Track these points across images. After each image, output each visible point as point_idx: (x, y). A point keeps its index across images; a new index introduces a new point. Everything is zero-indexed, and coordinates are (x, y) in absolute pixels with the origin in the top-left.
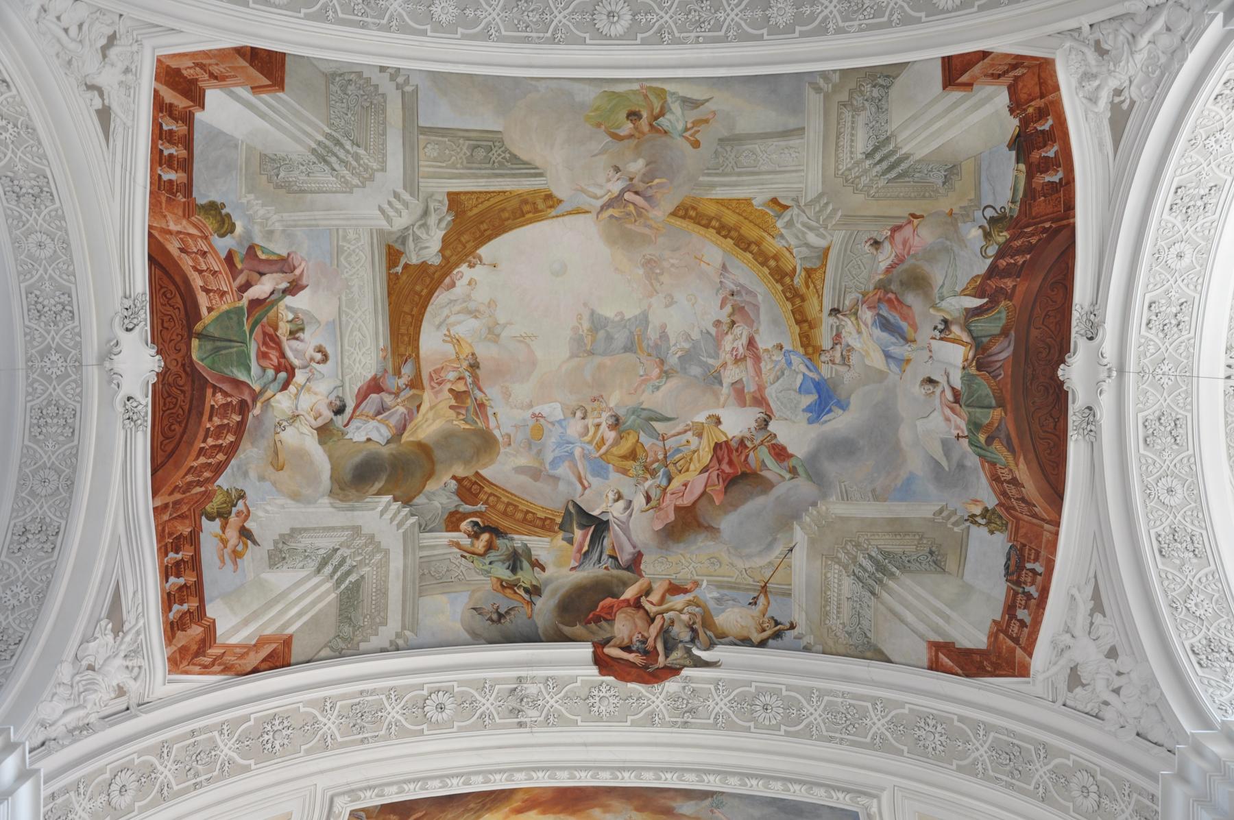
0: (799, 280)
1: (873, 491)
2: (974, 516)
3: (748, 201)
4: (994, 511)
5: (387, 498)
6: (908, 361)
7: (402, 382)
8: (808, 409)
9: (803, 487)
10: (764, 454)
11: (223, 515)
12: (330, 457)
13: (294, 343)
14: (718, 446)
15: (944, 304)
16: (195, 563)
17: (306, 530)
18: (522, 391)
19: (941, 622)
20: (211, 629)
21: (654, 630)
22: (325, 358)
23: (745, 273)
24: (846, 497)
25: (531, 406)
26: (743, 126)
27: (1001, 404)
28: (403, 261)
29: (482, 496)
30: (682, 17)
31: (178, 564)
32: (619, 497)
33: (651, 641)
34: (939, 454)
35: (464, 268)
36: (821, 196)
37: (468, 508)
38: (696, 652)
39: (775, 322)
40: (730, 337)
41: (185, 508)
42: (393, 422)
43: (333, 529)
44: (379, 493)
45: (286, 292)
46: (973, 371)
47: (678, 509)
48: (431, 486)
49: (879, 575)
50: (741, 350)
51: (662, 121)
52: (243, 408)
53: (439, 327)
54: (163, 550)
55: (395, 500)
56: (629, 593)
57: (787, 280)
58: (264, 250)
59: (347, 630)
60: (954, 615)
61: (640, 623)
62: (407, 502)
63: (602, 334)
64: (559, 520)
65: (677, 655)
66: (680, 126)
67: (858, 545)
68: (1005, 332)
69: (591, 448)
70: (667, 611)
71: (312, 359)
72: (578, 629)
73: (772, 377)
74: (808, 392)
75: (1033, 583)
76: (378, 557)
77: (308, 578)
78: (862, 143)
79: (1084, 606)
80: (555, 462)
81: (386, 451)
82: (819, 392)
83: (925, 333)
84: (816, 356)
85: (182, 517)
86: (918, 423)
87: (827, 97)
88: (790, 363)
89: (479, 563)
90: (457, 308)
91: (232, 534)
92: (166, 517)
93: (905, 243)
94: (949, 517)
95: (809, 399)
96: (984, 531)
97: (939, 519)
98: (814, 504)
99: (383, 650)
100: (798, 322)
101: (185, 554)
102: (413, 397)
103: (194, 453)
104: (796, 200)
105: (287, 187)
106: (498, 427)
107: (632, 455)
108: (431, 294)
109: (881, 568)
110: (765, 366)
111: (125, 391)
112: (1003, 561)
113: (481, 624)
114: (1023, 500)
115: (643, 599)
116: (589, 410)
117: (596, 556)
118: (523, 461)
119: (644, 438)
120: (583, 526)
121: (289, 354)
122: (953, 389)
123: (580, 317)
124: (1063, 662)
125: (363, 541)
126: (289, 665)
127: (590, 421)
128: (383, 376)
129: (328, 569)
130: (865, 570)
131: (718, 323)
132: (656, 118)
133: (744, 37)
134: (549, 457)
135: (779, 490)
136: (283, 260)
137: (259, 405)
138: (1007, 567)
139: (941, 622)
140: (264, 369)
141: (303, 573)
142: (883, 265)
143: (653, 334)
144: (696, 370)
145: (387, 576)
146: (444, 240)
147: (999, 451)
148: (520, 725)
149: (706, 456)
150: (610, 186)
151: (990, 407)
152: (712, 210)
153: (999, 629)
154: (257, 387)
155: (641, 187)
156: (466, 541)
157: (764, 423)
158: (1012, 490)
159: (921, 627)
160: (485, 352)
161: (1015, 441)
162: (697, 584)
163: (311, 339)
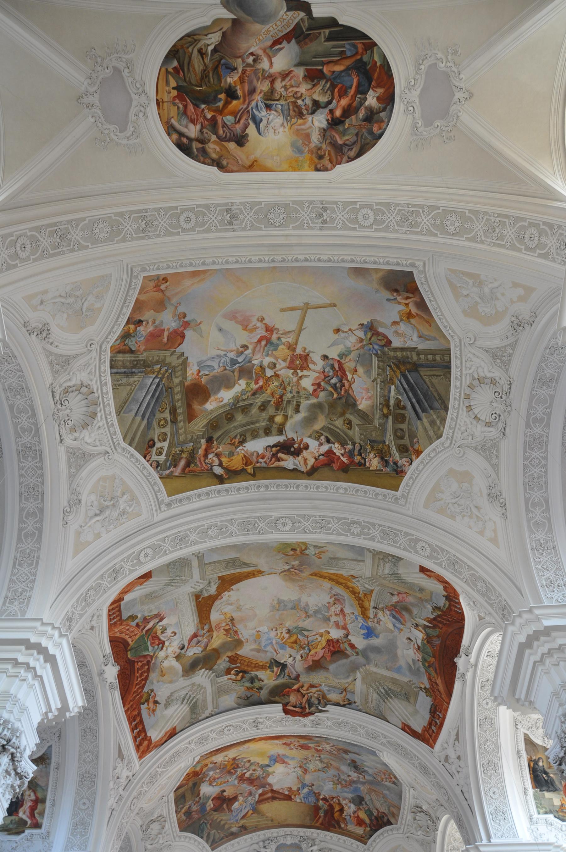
0: (361, 595)
1: (387, 667)
2: (421, 688)
3: (342, 575)
4: (428, 689)
5: (204, 670)
6: (402, 630)
7: (204, 632)
8: (363, 634)
9: (360, 659)
10: (346, 645)
11: (147, 701)
12: (181, 665)
13: (164, 635)
14: (328, 641)
15: (416, 619)
16: (141, 722)
17: (175, 691)
18: (251, 625)
19: (406, 718)
20: (150, 740)
21: (304, 700)
22: (175, 634)
23: (339, 590)
24: (376, 666)
25: (255, 628)
26: (339, 555)
27: (434, 657)
28: (202, 597)
29: (239, 661)
30: (314, 525)
31: (136, 725)
32: (291, 656)
33: (303, 704)
34: (411, 663)
35: (226, 593)
36: (370, 578)
37: (234, 666)
38: (320, 708)
39: (352, 606)
40: (333, 607)
41: (135, 706)
42: (203, 645)
43: (185, 687)
44: (200, 669)
45: (158, 622)
46: (425, 642)
47: (313, 661)
48: (219, 662)
49: (387, 696)
50: (338, 612)
51: (306, 552)
52: (148, 663)
53: (217, 611)
54: (130, 724)
55: (206, 670)
56: (295, 687)
57: (357, 595)
58: (148, 616)
59: (194, 716)
60: (411, 719)
61: (300, 697)
62: (211, 669)
63: (282, 604)
64: (268, 665)
65: (313, 709)
66: (313, 553)
67: (380, 683)
68: (438, 636)
69: (279, 640)
70: (309, 693)
71: (171, 636)
72: (277, 699)
73: (350, 622)
74: (364, 629)
75: (438, 719)
76: (202, 690)
77: (179, 707)
78: (387, 571)
79: (453, 737)
80: (265, 646)
81: (201, 655)
82: (368, 630)
83: (409, 624)
84: (367, 619)
85: (134, 709)
86: (405, 650)
87: (374, 555)
88: (357, 619)
89: (239, 684)
90: (224, 604)
91: (151, 705)
92: (129, 713)
93: (403, 598)
94: (413, 684)
95: (365, 631)
96: (424, 694)
97: (409, 684)
98: (365, 665)
99: (207, 718)
100: (360, 607)
101: (138, 720)
102: (209, 635)
103: (134, 686)
104: (361, 577)
105: (156, 597)
106: (243, 637)
107: (295, 642)
108: (213, 602)
109: (387, 693)
110: (347, 618)
111: (109, 681)
112: (430, 707)
113: (240, 701)
114: (438, 690)
115: (300, 689)
116: (278, 627)
117: (282, 676)
118: (254, 646)
119: (300, 637)
120: (276, 666)
121: (162, 638)
122: (418, 645)
123: (273, 600)
124: (443, 753)
125: (196, 687)
126: (176, 734)
127: (279, 632)
128: (197, 632)
129: (186, 701)
130: (382, 693)
131: (329, 603)
132: (303, 551)
133: (339, 534)
134: (263, 644)
135: (352, 658)
136: (156, 615)
137: (154, 659)
138: (431, 710)
139: (406, 718)
140: (154, 647)
141: (177, 706)
142: (394, 601)
143: (303, 604)
144: (320, 616)
145: (206, 696)
146: (217, 587)
147: (432, 671)
148: (257, 729)
149: (324, 643)
150: (284, 567)
151: (430, 656)
152: (327, 575)
153: (425, 729)
154: (152, 654)
155: (297, 568)
156: (233, 677)
157: (347, 636)
158: (435, 686)
159: (400, 717)
160: (235, 615)
161: (438, 671)
162: (320, 685)
163: (169, 632)
